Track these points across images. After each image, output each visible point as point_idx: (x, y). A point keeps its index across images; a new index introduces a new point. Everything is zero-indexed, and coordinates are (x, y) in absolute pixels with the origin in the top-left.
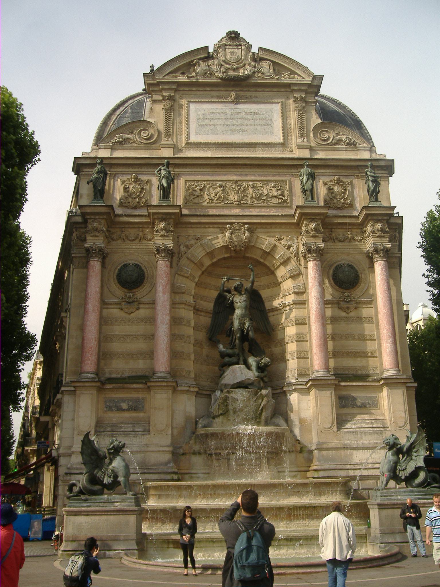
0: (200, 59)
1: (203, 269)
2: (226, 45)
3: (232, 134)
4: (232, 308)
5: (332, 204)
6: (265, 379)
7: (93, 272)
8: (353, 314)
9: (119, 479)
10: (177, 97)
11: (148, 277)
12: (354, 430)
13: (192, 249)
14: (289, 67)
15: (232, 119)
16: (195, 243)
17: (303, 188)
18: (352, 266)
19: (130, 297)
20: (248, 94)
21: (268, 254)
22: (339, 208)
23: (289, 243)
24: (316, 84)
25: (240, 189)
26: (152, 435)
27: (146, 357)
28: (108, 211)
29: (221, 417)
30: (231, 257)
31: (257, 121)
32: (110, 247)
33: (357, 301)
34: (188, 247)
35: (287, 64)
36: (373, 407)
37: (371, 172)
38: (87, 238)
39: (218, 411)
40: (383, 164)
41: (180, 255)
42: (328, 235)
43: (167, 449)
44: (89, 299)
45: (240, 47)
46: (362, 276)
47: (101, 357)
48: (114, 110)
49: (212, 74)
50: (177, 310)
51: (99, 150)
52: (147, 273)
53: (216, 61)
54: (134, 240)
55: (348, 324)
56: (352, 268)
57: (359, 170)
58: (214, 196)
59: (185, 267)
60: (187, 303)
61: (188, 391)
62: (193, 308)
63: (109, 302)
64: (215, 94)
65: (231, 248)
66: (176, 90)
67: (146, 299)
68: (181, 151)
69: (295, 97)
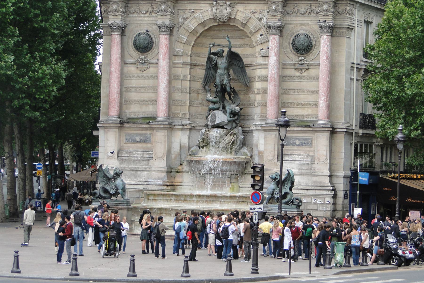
1: (198, 35)
6: (236, 121)
7: (114, 43)
8: (305, 74)
9: (119, 191)
11: (156, 43)
13: (188, 20)
19: (142, 59)
23: (261, 16)
26: (154, 160)
30: (219, 25)
32: (128, 19)
34: (185, 19)
36: (308, 146)
38: (110, 17)
41: (179, 26)
43: (163, 169)
44: (113, 63)
47: (123, 103)
50: (177, 69)
52: (155, 39)
54: (145, 13)
55: (300, 81)
56: (307, 37)
59: (182, 35)
60: (184, 63)
61: (182, 129)
62: (189, 66)
63: (128, 63)
67: (154, 60)
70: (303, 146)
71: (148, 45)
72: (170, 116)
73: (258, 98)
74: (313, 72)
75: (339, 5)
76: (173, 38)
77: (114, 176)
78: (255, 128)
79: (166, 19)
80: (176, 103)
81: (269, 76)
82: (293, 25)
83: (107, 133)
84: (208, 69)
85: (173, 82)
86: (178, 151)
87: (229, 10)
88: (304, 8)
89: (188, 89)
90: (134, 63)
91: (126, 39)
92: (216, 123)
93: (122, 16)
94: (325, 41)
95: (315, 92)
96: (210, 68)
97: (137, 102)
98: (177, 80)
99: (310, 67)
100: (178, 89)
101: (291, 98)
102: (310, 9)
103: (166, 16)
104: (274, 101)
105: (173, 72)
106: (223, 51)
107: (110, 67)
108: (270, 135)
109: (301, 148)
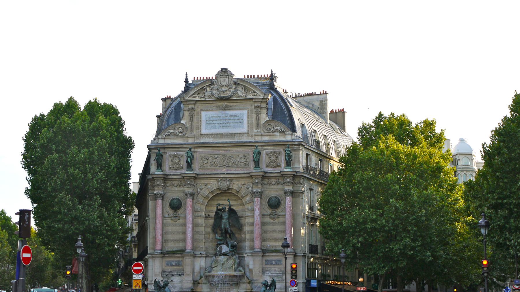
1: (209, 199)
3: (223, 128)
4: (221, 218)
8: (276, 221)
10: (196, 107)
14: (253, 89)
16: (205, 187)
17: (254, 160)
18: (277, 197)
19: (175, 214)
20: (232, 104)
21: (239, 192)
23: (248, 187)
28: (163, 176)
31: (235, 121)
37: (287, 151)
40: (297, 143)
43: (191, 282)
45: (228, 76)
46: (282, 202)
47: (164, 242)
49: (213, 95)
50: (196, 220)
56: (277, 199)
61: (201, 256)
62: (204, 218)
64: (215, 105)
67: (182, 215)
68: (197, 138)
69: (255, 106)
72: (194, 249)
73: (248, 236)
74: (281, 219)
75: (295, 178)
76: (194, 201)
78: (246, 255)
81: (255, 222)
83: (155, 260)
85: (194, 228)
86: (199, 270)
87: (228, 183)
89: (204, 232)
91: (164, 202)
93: (162, 188)
94: (288, 201)
98: (197, 226)
99: (279, 217)
100: (198, 232)
101: (268, 236)
105: (194, 222)
106: (226, 208)
107: (156, 220)
109: (275, 266)
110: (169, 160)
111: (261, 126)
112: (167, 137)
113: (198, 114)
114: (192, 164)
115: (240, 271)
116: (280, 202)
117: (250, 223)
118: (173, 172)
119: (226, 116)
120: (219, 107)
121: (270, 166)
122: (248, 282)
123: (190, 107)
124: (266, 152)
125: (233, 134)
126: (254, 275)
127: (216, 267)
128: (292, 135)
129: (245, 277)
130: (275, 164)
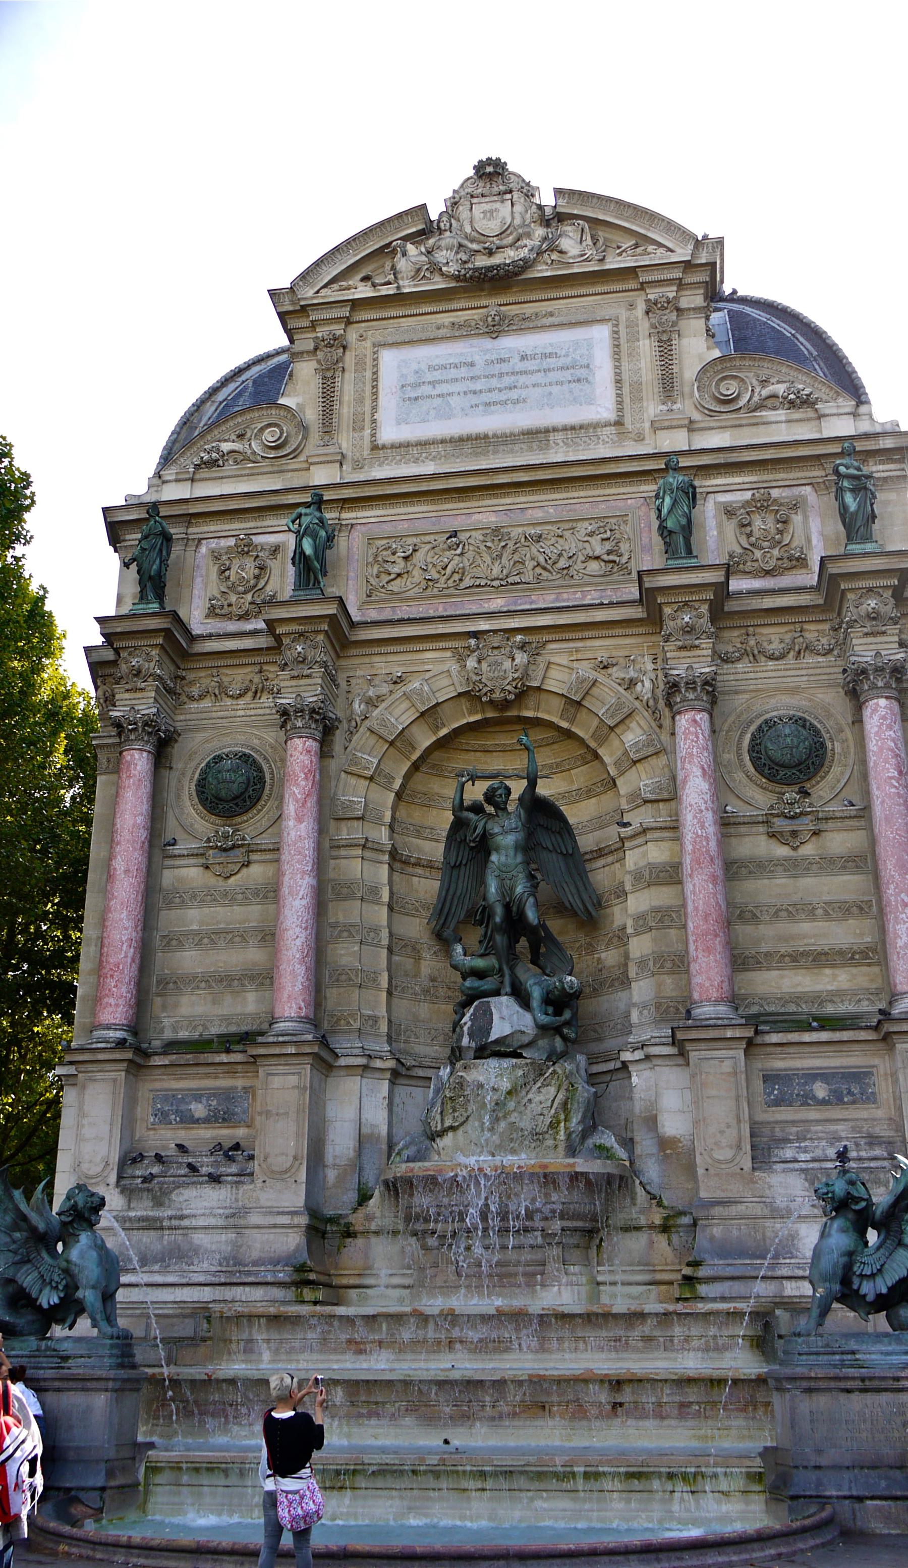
0: (405, 239)
1: (415, 756)
2: (472, 196)
5: (749, 564)
6: (565, 1031)
8: (808, 850)
9: (80, 1294)
10: (352, 335)
11: (272, 785)
12: (803, 1165)
13: (383, 706)
14: (634, 228)
15: (486, 377)
17: (662, 528)
18: (805, 720)
19: (226, 837)
20: (529, 309)
21: (579, 704)
22: (768, 573)
23: (632, 674)
24: (704, 261)
25: (503, 547)
26: (259, 1183)
27: (263, 984)
29: (450, 1134)
32: (182, 717)
33: (821, 815)
34: (371, 703)
35: (627, 221)
36: (864, 1102)
37: (847, 467)
39: (442, 1120)
40: (888, 443)
41: (354, 723)
42: (739, 645)
45: (508, 196)
47: (154, 989)
48: (213, 391)
49: (434, 268)
51: (165, 486)
52: (272, 773)
53: (448, 239)
54: (240, 696)
55: (795, 877)
56: (804, 726)
57: (825, 469)
58: (439, 572)
60: (369, 845)
61: (366, 1067)
64: (446, 319)
65: (480, 698)
66: (349, 322)
67: (264, 841)
68: (358, 466)
69: (648, 301)
70: (845, 1103)
71: (246, 789)
76: (333, 765)
77: (64, 1224)
78: (638, 1055)
79: (309, 688)
80: (343, 977)
82: (747, 696)
83: (84, 1087)
84: (451, 868)
86: (352, 1154)
87: (521, 658)
88: (778, 641)
89: (385, 933)
90: (195, 852)
92: (494, 1035)
93: (157, 691)
95: (855, 910)
96: (456, 867)
97: (203, 985)
98: (345, 899)
99: (823, 826)
100: (349, 929)
102: (801, 639)
103: (308, 676)
104: (716, 935)
105: (332, 875)
108: (716, 1062)
109: (836, 1113)
110: (207, 576)
111: (686, 390)
112: (204, 473)
113: (360, 364)
114: (325, 574)
115: (603, 1151)
116: (823, 745)
117: (651, 867)
118: (232, 626)
119: (502, 361)
120: (466, 324)
121: (749, 566)
122: (658, 1221)
123: (322, 332)
124: (719, 503)
125: (538, 432)
126: (700, 1171)
127: (452, 1128)
128: (855, 415)
129: (639, 1190)
130: (776, 552)
